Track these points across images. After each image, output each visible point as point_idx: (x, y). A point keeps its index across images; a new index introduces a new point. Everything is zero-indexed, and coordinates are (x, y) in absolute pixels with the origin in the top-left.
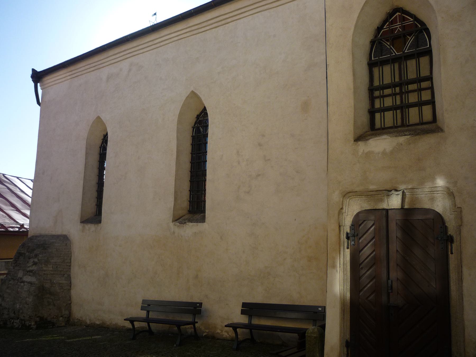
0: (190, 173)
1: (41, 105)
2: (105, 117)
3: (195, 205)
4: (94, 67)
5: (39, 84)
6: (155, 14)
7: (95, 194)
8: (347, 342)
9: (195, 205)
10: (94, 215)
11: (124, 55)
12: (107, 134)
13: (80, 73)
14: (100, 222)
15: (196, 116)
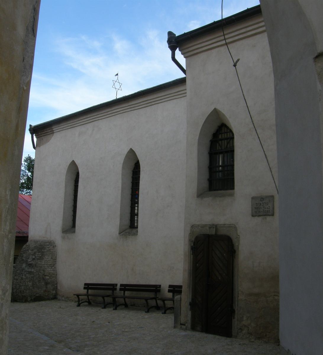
0: (130, 201)
1: (36, 149)
2: (78, 162)
3: (131, 224)
4: (71, 126)
5: (34, 135)
6: (117, 75)
7: (72, 213)
8: (190, 303)
9: (131, 224)
10: (71, 226)
11: (90, 120)
12: (79, 172)
13: (62, 129)
14: (74, 232)
15: (134, 164)
